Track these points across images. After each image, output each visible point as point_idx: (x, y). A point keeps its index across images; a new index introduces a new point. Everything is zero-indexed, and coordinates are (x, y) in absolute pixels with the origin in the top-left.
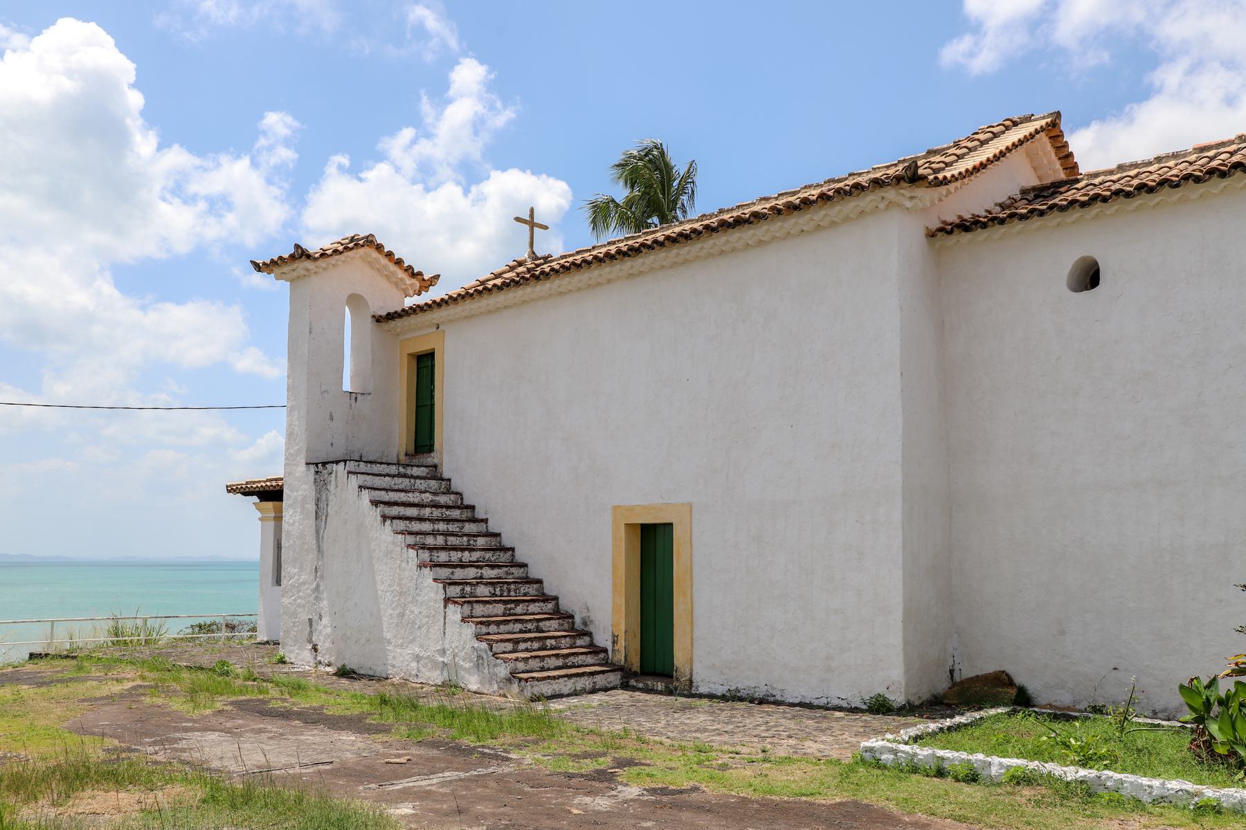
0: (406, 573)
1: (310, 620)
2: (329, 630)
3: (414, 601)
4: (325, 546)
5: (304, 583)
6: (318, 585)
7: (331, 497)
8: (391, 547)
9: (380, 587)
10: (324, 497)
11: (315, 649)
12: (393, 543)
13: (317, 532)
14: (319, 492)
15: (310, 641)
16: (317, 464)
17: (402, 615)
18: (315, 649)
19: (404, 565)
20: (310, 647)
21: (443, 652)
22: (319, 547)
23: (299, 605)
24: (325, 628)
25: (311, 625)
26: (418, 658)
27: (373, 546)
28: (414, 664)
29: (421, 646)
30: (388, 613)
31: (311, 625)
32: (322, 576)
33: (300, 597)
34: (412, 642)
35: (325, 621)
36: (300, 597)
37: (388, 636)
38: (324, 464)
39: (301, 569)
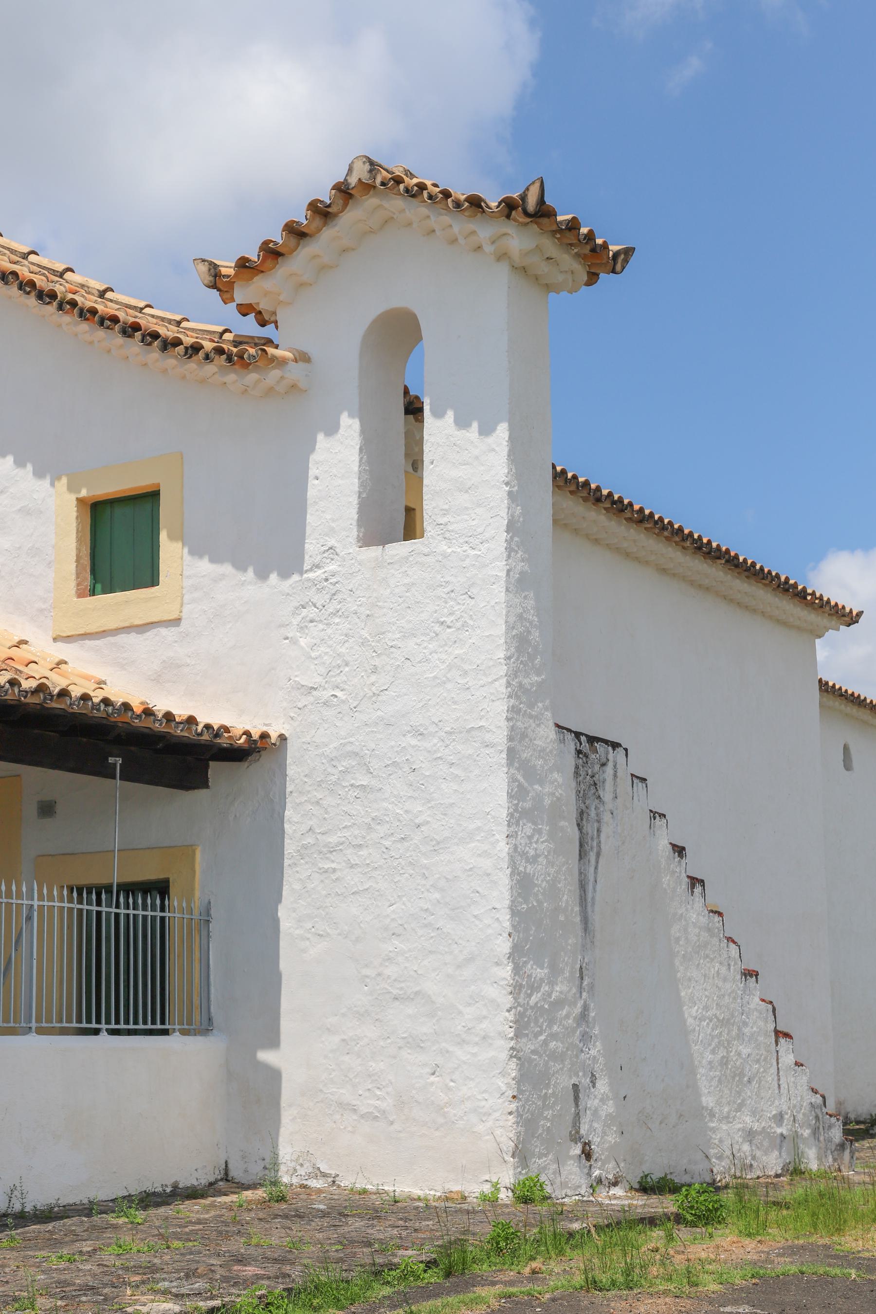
0: (728, 985)
1: (575, 1087)
2: (610, 1108)
3: (740, 1036)
4: (596, 918)
5: (559, 1004)
6: (585, 1008)
7: (606, 817)
8: (705, 935)
9: (691, 1013)
10: (593, 813)
11: (587, 1154)
12: (709, 930)
13: (583, 886)
14: (581, 796)
15: (575, 1137)
16: (578, 735)
17: (724, 1062)
18: (587, 1154)
19: (724, 970)
20: (577, 1150)
21: (779, 1118)
22: (585, 920)
23: (554, 1056)
24: (601, 1101)
25: (576, 1099)
26: (750, 1135)
27: (675, 930)
28: (746, 1147)
29: (754, 1113)
30: (705, 1057)
31: (576, 1099)
32: (592, 987)
33: (553, 1036)
34: (739, 1108)
35: (603, 1086)
36: (553, 1036)
37: (708, 1101)
38: (592, 740)
39: (555, 970)
